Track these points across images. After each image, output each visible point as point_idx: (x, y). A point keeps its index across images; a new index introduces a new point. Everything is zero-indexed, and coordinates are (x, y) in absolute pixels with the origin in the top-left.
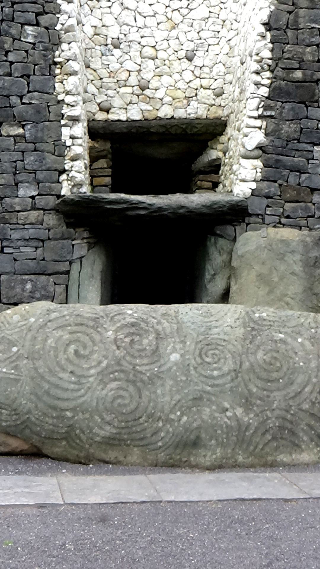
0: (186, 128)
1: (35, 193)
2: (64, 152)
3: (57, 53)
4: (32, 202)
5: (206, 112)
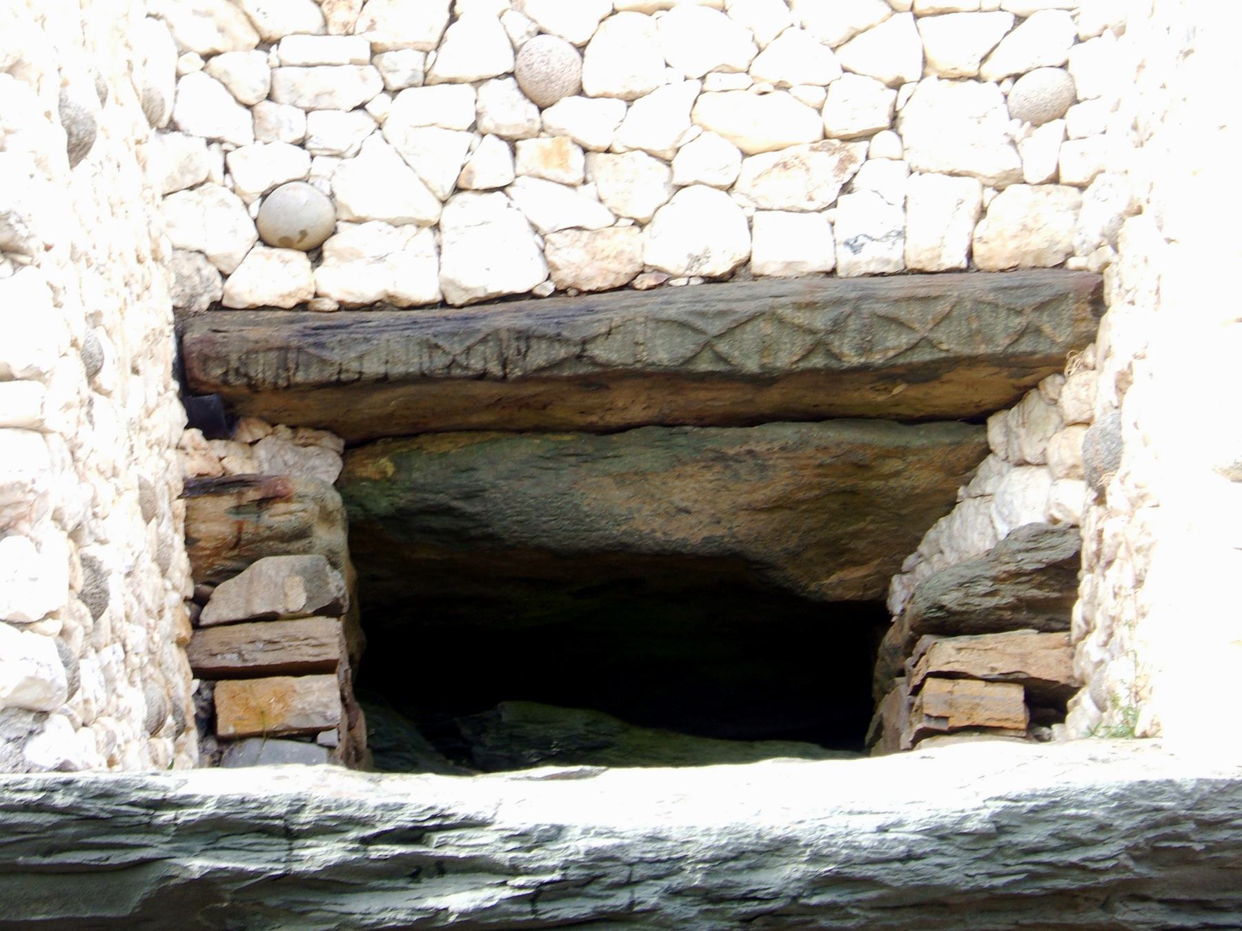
0: (837, 327)
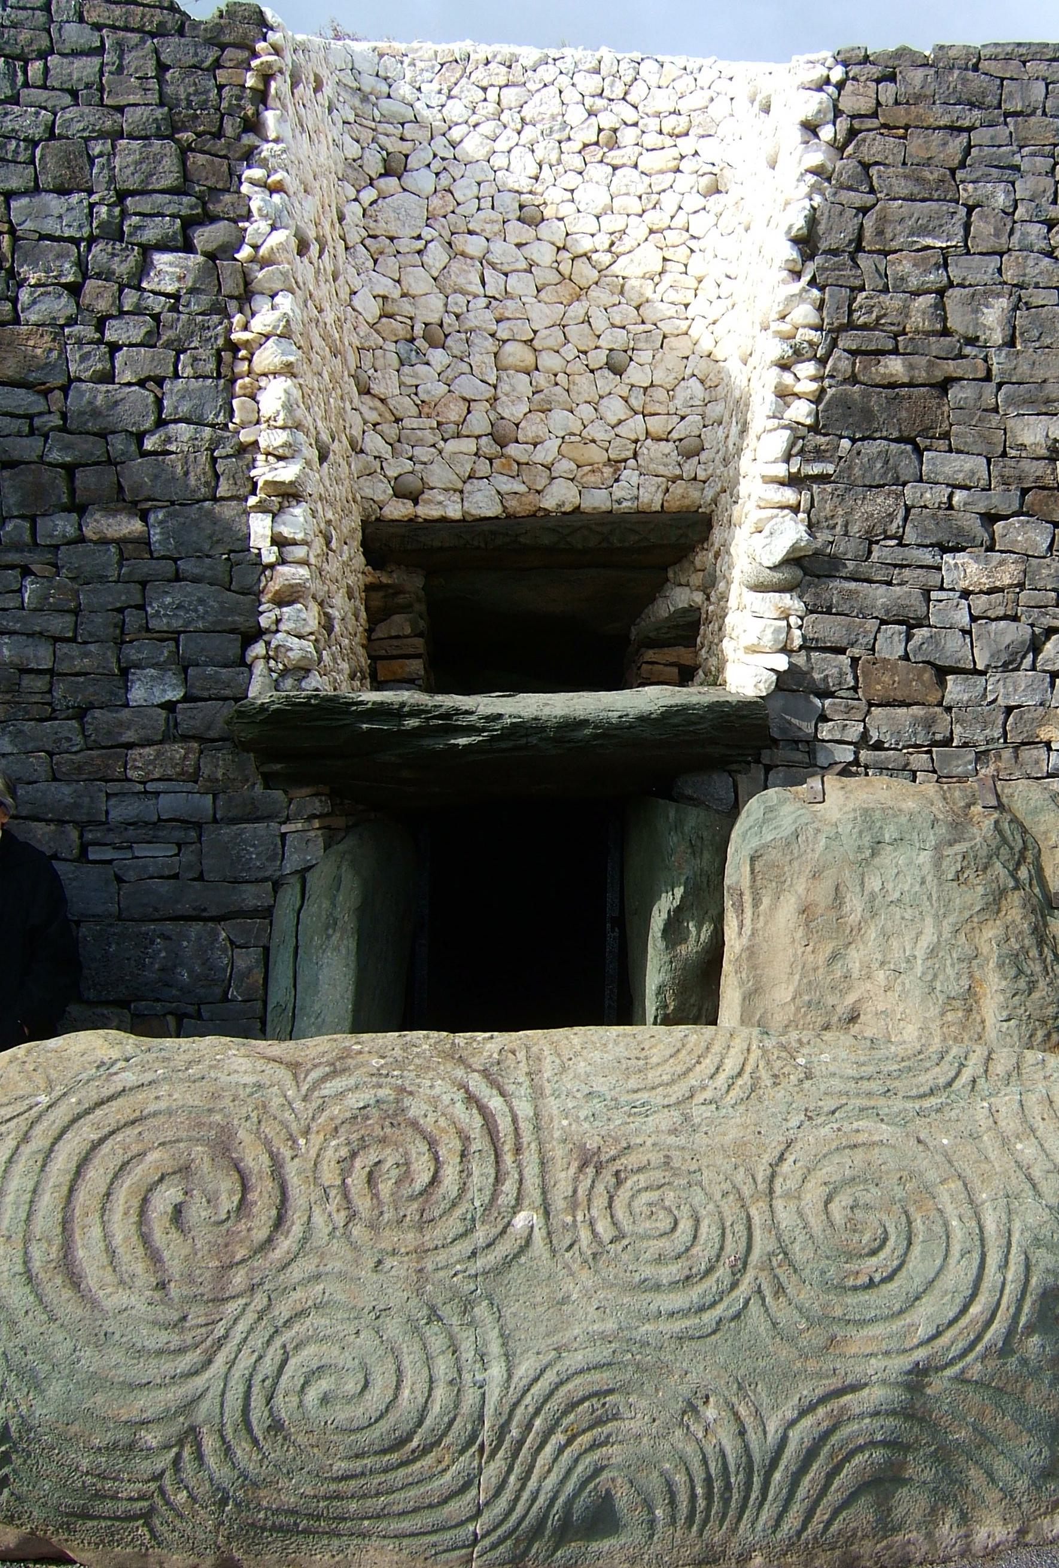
1: (174, 694)
2: (259, 580)
3: (238, 319)
4: (167, 720)
5: (659, 496)
